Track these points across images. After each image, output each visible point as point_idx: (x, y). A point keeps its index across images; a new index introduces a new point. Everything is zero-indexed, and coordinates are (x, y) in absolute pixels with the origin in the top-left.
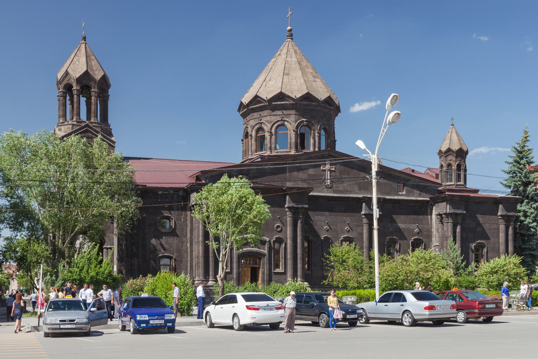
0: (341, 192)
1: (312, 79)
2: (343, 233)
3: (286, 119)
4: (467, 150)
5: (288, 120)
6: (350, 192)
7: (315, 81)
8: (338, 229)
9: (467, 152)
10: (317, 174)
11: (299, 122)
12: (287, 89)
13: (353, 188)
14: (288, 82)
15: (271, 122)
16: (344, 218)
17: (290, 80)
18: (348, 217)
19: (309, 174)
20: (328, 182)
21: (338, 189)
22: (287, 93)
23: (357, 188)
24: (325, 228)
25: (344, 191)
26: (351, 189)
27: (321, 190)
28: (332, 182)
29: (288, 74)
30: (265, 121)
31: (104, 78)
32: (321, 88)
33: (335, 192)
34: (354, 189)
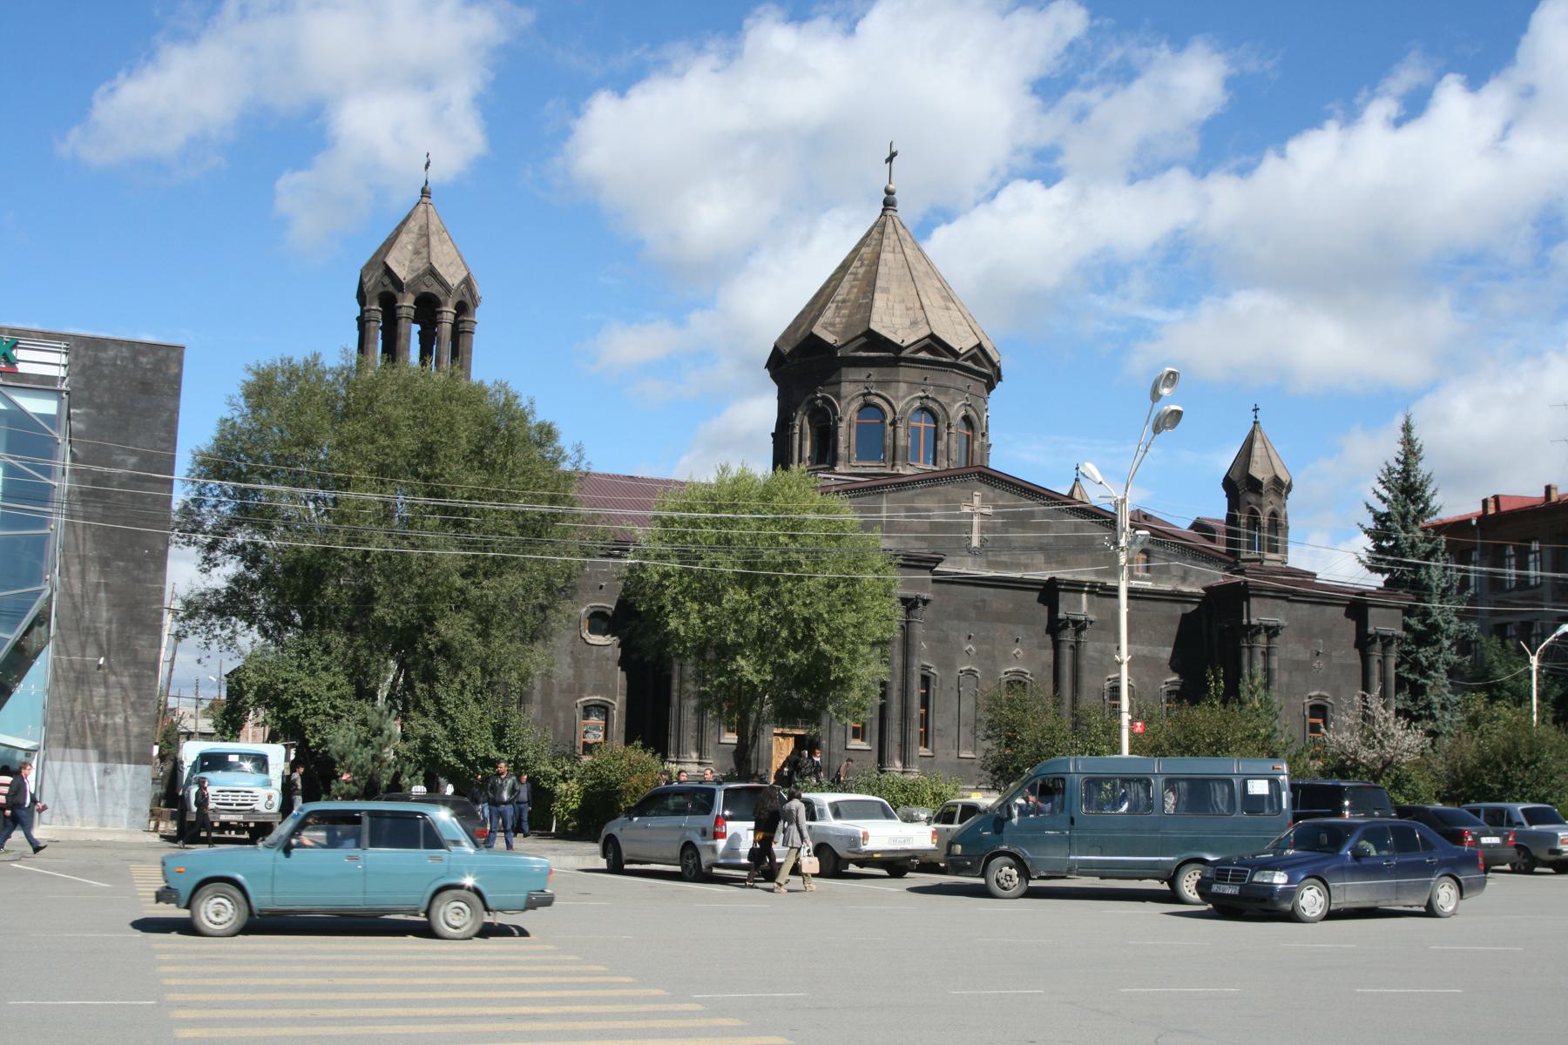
0: (1006, 566)
1: (942, 303)
2: (1008, 662)
3: (879, 392)
4: (1290, 483)
5: (883, 394)
6: (1026, 567)
7: (948, 309)
8: (997, 653)
9: (1289, 488)
11: (908, 399)
15: (846, 397)
17: (890, 304)
18: (1021, 626)
22: (884, 333)
24: (967, 648)
25: (1012, 564)
29: (886, 290)
30: (831, 394)
31: (467, 282)
32: (961, 324)
33: (991, 565)
34: (1035, 561)
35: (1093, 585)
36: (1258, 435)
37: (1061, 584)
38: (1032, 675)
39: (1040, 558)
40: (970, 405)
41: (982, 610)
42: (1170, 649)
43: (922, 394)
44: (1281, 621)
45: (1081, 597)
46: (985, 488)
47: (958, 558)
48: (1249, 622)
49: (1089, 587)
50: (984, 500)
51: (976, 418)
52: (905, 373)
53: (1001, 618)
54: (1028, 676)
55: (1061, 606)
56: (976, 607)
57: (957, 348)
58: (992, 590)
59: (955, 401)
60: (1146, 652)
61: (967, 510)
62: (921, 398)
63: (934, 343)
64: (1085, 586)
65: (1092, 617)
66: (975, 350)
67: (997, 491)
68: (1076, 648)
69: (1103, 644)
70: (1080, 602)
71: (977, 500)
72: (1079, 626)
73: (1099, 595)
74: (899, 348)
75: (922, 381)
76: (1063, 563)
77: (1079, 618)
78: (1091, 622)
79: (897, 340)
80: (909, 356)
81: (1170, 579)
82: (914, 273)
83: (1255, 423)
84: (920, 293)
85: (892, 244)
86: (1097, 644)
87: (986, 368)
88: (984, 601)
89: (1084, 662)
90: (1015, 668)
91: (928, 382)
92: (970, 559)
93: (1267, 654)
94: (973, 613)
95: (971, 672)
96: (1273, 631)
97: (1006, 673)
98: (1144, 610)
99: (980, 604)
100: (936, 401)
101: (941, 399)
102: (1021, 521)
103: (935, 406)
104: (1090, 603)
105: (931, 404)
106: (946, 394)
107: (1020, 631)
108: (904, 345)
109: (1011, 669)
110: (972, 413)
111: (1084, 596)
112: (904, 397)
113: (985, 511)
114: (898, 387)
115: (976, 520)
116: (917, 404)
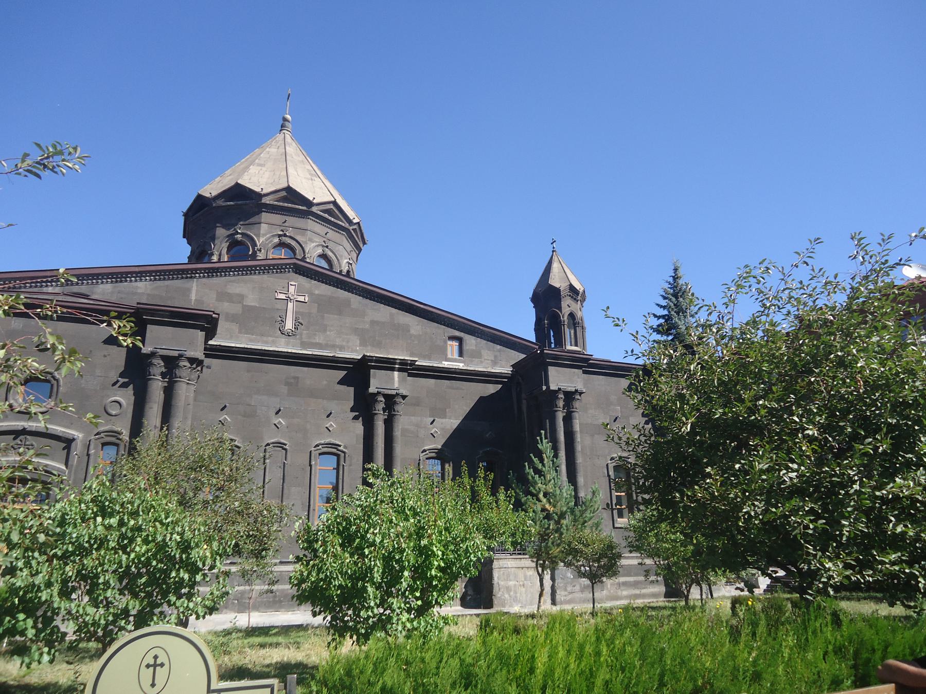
6: (342, 348)
10: (264, 306)
11: (268, 236)
12: (251, 181)
13: (348, 342)
14: (257, 172)
16: (325, 402)
17: (261, 172)
18: (336, 401)
19: (245, 305)
20: (289, 325)
21: (314, 341)
23: (358, 342)
26: (344, 344)
27: (273, 341)
28: (298, 324)
32: (321, 188)
33: (304, 345)
35: (403, 363)
36: (555, 258)
37: (371, 361)
38: (345, 447)
39: (355, 341)
40: (327, 247)
41: (293, 386)
43: (281, 233)
44: (580, 387)
45: (393, 374)
46: (303, 280)
47: (270, 339)
48: (548, 387)
49: (400, 364)
50: (300, 291)
51: (334, 258)
52: (265, 216)
53: (313, 394)
54: (341, 448)
55: (372, 381)
56: (287, 384)
57: (311, 199)
58: (306, 369)
59: (311, 240)
61: (283, 296)
62: (280, 236)
63: (291, 194)
64: (395, 363)
65: (403, 392)
66: (331, 206)
67: (313, 282)
68: (389, 424)
69: (419, 418)
70: (393, 379)
71: (292, 289)
72: (391, 401)
73: (410, 375)
74: (259, 196)
75: (281, 224)
76: (378, 345)
77: (390, 392)
78: (404, 397)
79: (257, 189)
80: (268, 202)
81: (481, 362)
82: (288, 157)
83: (553, 251)
84: (288, 167)
85: (278, 145)
86: (413, 418)
87: (342, 221)
88: (296, 378)
89: (398, 433)
90: (327, 441)
91: (286, 224)
92: (283, 340)
93: (568, 420)
94: (284, 389)
95: (281, 445)
96: (570, 396)
97: (317, 446)
98: (457, 388)
99: (292, 381)
100: (291, 237)
101: (298, 238)
102: (341, 308)
103: (293, 243)
104: (401, 381)
105: (289, 241)
106: (303, 235)
107: (333, 406)
108: (265, 192)
109: (323, 442)
110: (330, 254)
111: (396, 373)
112: (264, 235)
113: (301, 299)
114: (259, 229)
115: (290, 305)
116: (276, 240)
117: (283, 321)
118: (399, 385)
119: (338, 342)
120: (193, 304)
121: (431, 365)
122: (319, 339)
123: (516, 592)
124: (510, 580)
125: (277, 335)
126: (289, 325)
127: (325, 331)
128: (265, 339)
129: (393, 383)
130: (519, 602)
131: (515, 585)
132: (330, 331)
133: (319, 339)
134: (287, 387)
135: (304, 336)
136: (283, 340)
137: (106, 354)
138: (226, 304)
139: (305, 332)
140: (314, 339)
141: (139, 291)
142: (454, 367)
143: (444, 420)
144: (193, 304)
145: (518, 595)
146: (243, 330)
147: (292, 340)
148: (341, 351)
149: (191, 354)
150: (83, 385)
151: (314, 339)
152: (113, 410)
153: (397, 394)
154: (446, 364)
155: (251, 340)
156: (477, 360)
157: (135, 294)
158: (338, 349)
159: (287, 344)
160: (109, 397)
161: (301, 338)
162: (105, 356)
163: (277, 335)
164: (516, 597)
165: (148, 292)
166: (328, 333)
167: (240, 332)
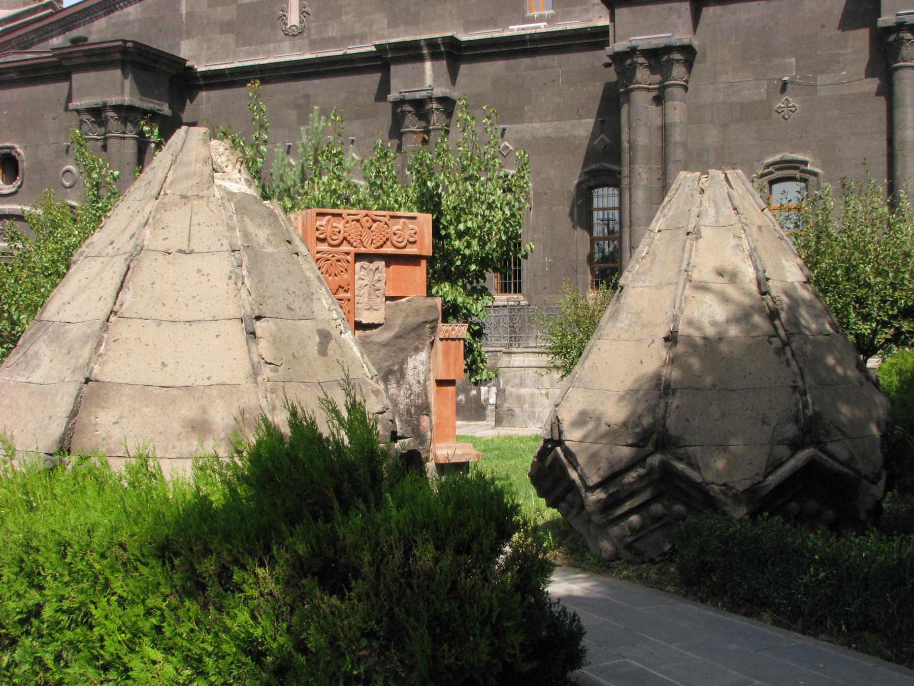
13: (371, 25)
18: (358, 122)
20: (294, 18)
21: (325, 35)
23: (385, 21)
25: (343, 38)
26: (366, 29)
27: (275, 48)
33: (313, 46)
34: (375, 27)
35: (431, 43)
39: (381, 21)
42: (591, 121)
47: (272, 46)
60: (549, 131)
70: (423, 72)
76: (414, 20)
77: (418, 96)
81: (587, 11)
92: (287, 43)
98: (545, 67)
99: (302, 101)
111: (428, 65)
117: (283, 18)
118: (434, 81)
119: (358, 29)
120: (184, 20)
121: (489, 36)
122: (333, 31)
123: (532, 405)
124: (526, 387)
125: (279, 38)
126: (294, 18)
127: (340, 15)
128: (266, 47)
129: (423, 80)
130: (538, 420)
131: (532, 395)
132: (347, 14)
133: (333, 31)
134: (295, 113)
135: (313, 31)
136: (287, 44)
137: (55, 115)
138: (219, 9)
139: (313, 25)
140: (326, 32)
141: (131, 18)
142: (529, 32)
143: (520, 126)
144: (184, 20)
145: (537, 410)
146: (241, 42)
147: (298, 41)
148: (361, 42)
149: (114, 100)
150: (41, 157)
151: (326, 32)
152: (67, 181)
153: (430, 99)
154: (515, 30)
155: (250, 54)
156: (578, 9)
157: (127, 23)
158: (357, 41)
159: (293, 49)
160: (63, 166)
161: (309, 35)
162: (54, 119)
163: (279, 38)
164: (533, 413)
165: (139, 16)
166: (344, 18)
167: (237, 46)
